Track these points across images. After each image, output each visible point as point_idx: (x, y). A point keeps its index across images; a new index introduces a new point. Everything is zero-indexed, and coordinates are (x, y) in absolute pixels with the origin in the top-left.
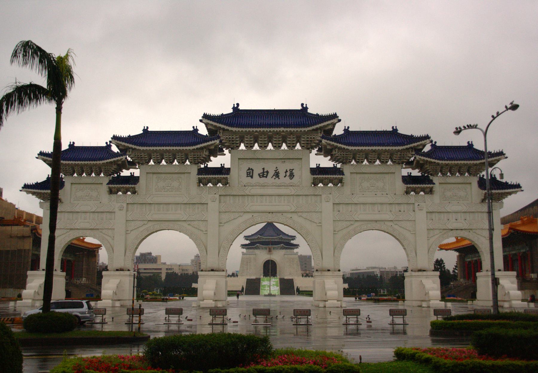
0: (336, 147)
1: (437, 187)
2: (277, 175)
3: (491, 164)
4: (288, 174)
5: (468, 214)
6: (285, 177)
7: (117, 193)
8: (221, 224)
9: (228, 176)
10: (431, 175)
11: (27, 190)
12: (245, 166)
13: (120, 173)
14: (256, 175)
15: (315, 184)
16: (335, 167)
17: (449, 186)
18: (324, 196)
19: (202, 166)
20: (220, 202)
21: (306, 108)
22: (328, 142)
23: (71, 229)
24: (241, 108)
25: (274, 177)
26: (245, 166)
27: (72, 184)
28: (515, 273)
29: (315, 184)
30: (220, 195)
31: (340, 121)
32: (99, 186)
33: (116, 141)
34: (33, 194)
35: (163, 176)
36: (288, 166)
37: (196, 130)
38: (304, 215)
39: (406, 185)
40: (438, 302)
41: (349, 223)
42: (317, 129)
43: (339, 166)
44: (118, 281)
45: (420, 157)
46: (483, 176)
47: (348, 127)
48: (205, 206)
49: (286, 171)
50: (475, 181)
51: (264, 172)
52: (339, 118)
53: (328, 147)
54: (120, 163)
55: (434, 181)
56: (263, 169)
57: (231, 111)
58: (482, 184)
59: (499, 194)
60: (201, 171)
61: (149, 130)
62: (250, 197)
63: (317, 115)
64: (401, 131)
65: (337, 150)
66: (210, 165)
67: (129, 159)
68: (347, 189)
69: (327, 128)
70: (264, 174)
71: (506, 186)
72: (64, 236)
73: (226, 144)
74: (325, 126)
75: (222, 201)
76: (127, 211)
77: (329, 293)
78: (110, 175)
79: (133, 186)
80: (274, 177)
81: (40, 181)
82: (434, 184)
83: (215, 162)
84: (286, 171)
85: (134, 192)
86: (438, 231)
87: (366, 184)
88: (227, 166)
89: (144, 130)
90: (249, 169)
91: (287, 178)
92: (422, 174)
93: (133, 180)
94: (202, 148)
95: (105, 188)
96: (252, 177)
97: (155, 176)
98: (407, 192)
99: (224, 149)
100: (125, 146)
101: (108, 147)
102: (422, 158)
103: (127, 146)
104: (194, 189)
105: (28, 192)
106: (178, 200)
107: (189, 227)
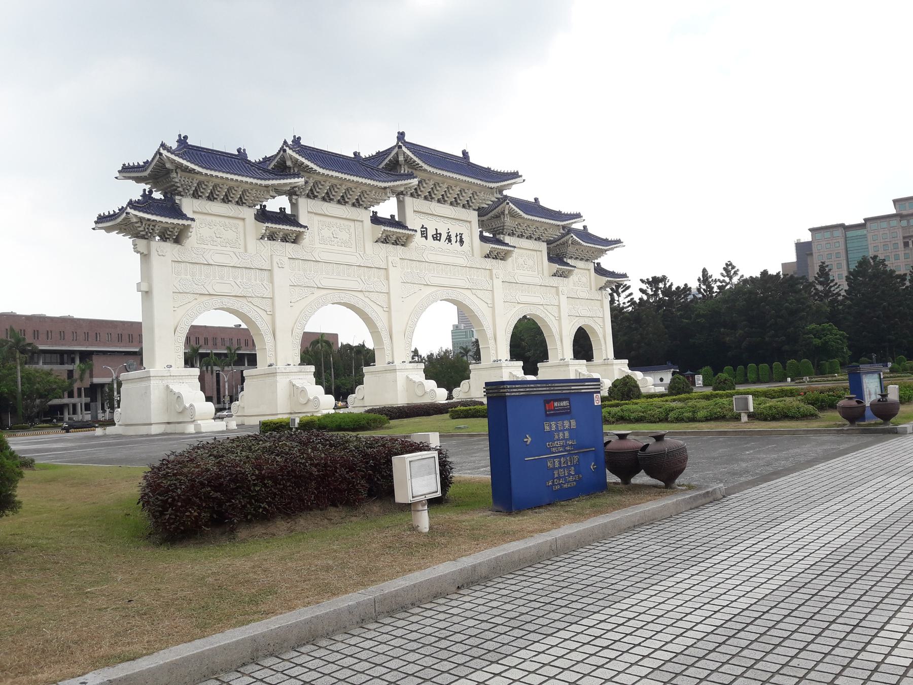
2: (449, 239)
13: (265, 206)
14: (430, 236)
28: (627, 361)
38: (479, 293)
39: (558, 266)
52: (523, 178)
63: (489, 169)
70: (437, 237)
94: (385, 188)
97: (317, 218)
104: (370, 246)
107: (367, 300)
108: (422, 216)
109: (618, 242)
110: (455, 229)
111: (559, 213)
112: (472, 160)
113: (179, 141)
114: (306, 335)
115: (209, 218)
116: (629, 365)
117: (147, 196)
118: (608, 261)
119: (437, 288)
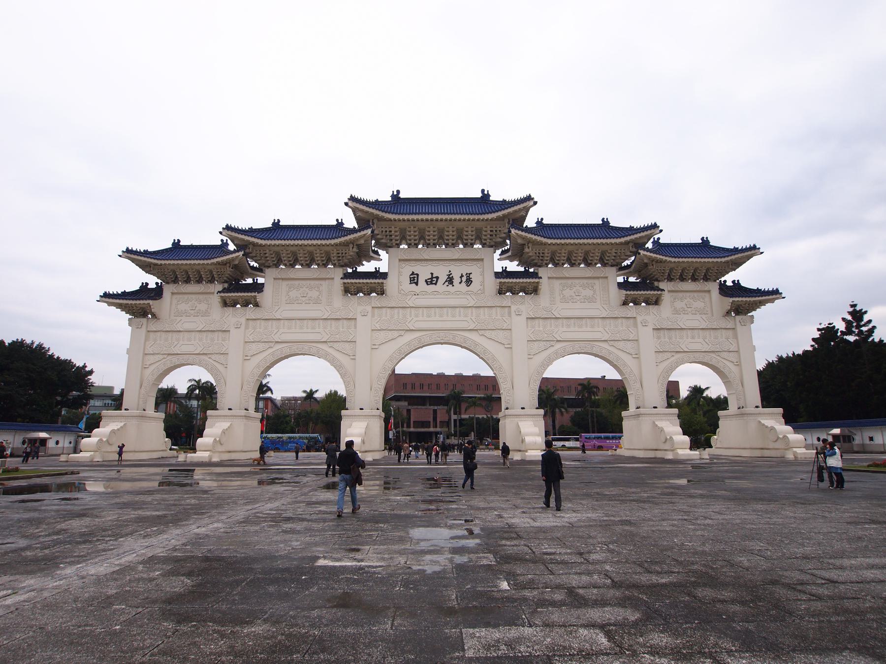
0: (530, 241)
1: (666, 297)
2: (450, 280)
3: (736, 265)
4: (464, 279)
5: (707, 332)
7: (234, 305)
9: (384, 281)
10: (657, 280)
11: (107, 300)
12: (408, 270)
13: (239, 281)
15: (501, 292)
16: (526, 272)
17: (680, 295)
18: (513, 308)
19: (350, 270)
20: (373, 316)
21: (488, 195)
22: (520, 233)
24: (402, 196)
26: (408, 270)
27: (173, 293)
28: (780, 410)
29: (501, 292)
31: (535, 203)
32: (211, 296)
33: (230, 233)
34: (119, 306)
35: (297, 282)
36: (464, 269)
37: (340, 224)
38: (487, 333)
39: (624, 292)
40: (688, 451)
42: (504, 216)
43: (531, 270)
44: (225, 425)
46: (725, 281)
47: (542, 219)
48: (353, 321)
49: (462, 276)
50: (714, 287)
51: (432, 278)
53: (520, 241)
54: (237, 262)
55: (661, 287)
56: (432, 274)
57: (390, 199)
58: (725, 290)
59: (749, 303)
60: (346, 276)
61: (281, 224)
62: (413, 310)
63: (504, 201)
64: (613, 223)
66: (360, 269)
67: (253, 264)
68: (544, 299)
69: (518, 215)
70: (432, 280)
71: (758, 292)
72: (157, 364)
73: (383, 241)
74: (515, 211)
76: (247, 328)
77: (528, 439)
78: (226, 282)
79: (253, 294)
81: (129, 289)
82: (663, 290)
83: (367, 267)
84: (462, 276)
85: (257, 305)
86: (669, 355)
87: (568, 292)
88: (384, 269)
89: (274, 224)
90: (413, 273)
91: (463, 284)
92: (643, 279)
93: (258, 288)
95: (216, 299)
96: (417, 284)
97: (285, 283)
98: (625, 303)
99: (380, 251)
100: (243, 240)
101: (224, 245)
102: (648, 254)
103: (248, 241)
105: (110, 304)
107: (331, 351)
108: (413, 263)
109: (752, 251)
110: (457, 271)
111: (631, 228)
112: (491, 198)
113: (174, 244)
114: (545, 380)
115: (186, 296)
116: (784, 416)
117: (144, 287)
118: (746, 275)
119: (424, 333)
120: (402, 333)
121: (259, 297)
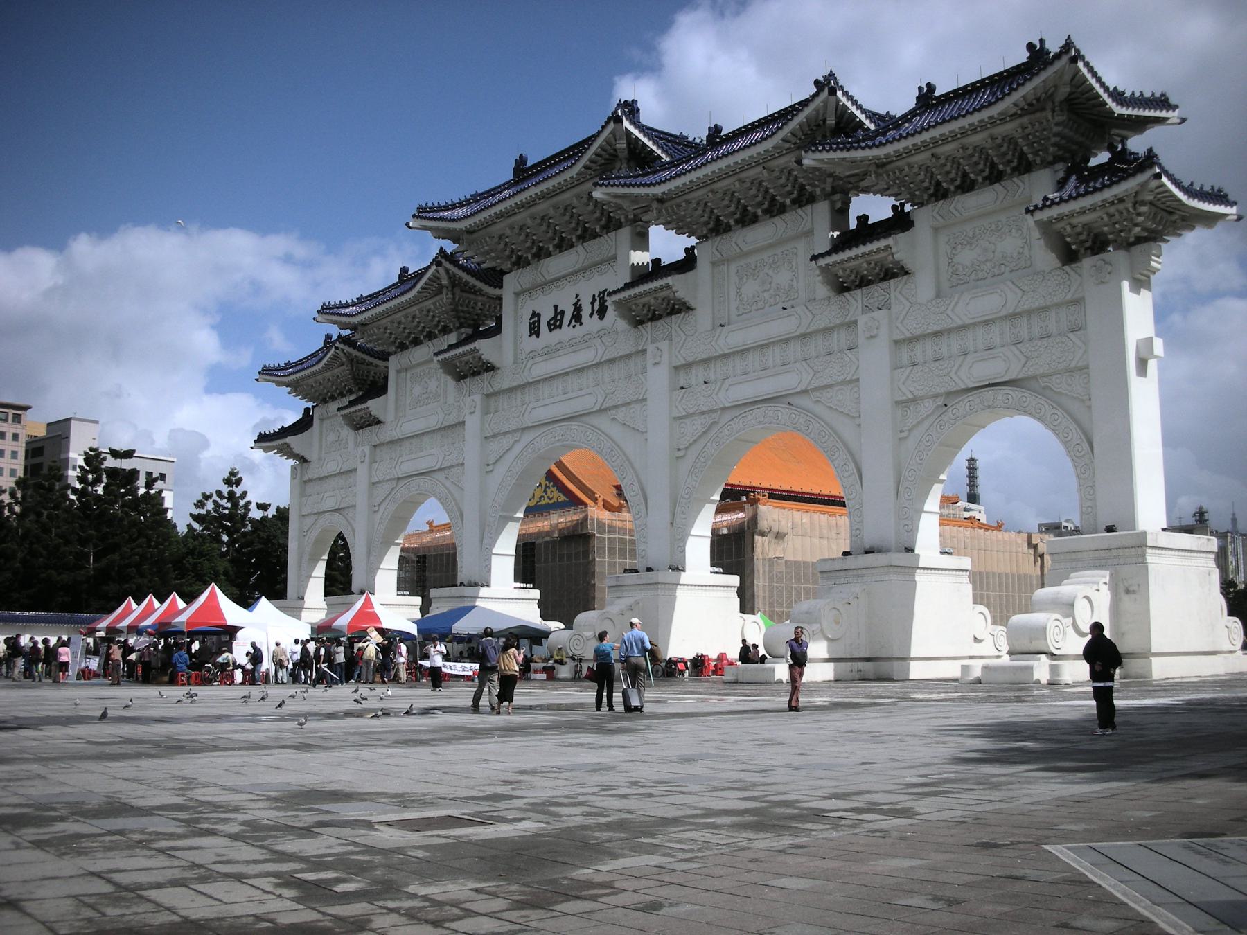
2: (577, 317)
6: (591, 316)
8: (490, 468)
18: (651, 348)
22: (610, 190)
23: (319, 513)
25: (573, 323)
30: (488, 396)
35: (418, 370)
38: (620, 414)
41: (707, 420)
45: (818, 156)
56: (556, 307)
65: (655, 205)
75: (492, 410)
76: (373, 461)
78: (360, 389)
80: (573, 323)
84: (594, 300)
87: (751, 287)
90: (534, 314)
91: (596, 316)
92: (894, 208)
105: (266, 450)
106: (433, 422)
120: (518, 435)
121: (374, 405)
